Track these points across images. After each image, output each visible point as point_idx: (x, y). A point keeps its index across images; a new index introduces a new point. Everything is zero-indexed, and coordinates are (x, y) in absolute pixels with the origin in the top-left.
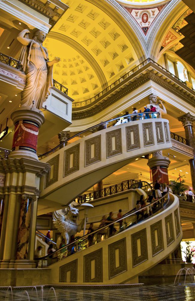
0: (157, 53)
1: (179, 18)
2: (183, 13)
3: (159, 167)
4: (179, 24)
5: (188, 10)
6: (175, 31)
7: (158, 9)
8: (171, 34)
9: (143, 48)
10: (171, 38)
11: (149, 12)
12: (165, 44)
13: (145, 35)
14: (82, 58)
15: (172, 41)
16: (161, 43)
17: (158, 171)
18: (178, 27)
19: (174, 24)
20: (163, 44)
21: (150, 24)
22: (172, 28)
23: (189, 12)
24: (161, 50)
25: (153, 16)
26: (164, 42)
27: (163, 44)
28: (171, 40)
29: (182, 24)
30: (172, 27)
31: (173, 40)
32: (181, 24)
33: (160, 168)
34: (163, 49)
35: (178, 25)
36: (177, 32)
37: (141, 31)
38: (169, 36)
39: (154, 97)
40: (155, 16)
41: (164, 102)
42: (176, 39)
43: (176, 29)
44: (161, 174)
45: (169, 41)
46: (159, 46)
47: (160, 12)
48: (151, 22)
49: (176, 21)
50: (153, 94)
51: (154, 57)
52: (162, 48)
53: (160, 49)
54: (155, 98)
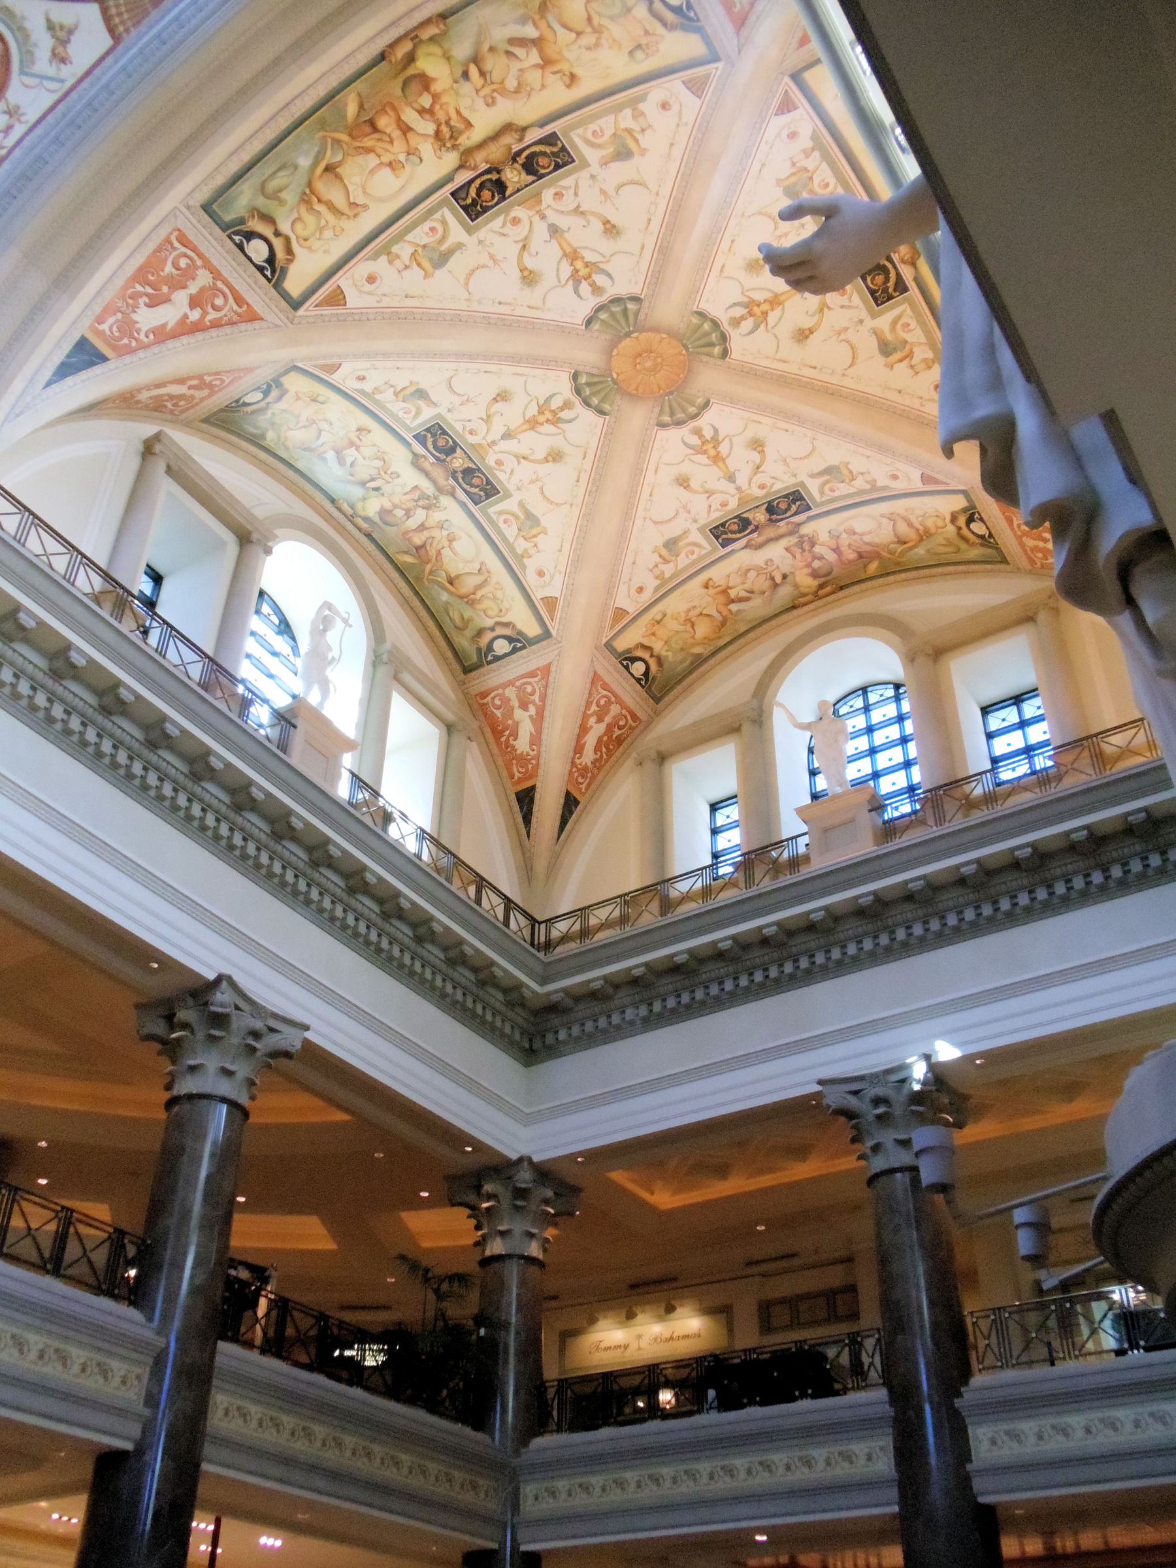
1: (270, 135)
2: (308, 102)
4: (275, 196)
5: (359, 85)
6: (241, 247)
7: (107, 19)
8: (192, 267)
10: (194, 302)
11: (27, 25)
12: (128, 327)
15: (198, 328)
16: (75, 308)
18: (269, 219)
19: (220, 180)
20: (100, 320)
21: (19, 130)
22: (206, 207)
23: (361, 107)
25: (51, 70)
26: (107, 311)
27: (100, 320)
28: (195, 315)
29: (305, 200)
30: (204, 195)
31: (216, 324)
32: (290, 196)
35: (261, 202)
36: (261, 269)
38: (169, 269)
40: (71, 73)
42: (243, 326)
43: (250, 235)
45: (168, 315)
47: (120, 48)
48: (32, 116)
49: (246, 157)
53: (58, 358)
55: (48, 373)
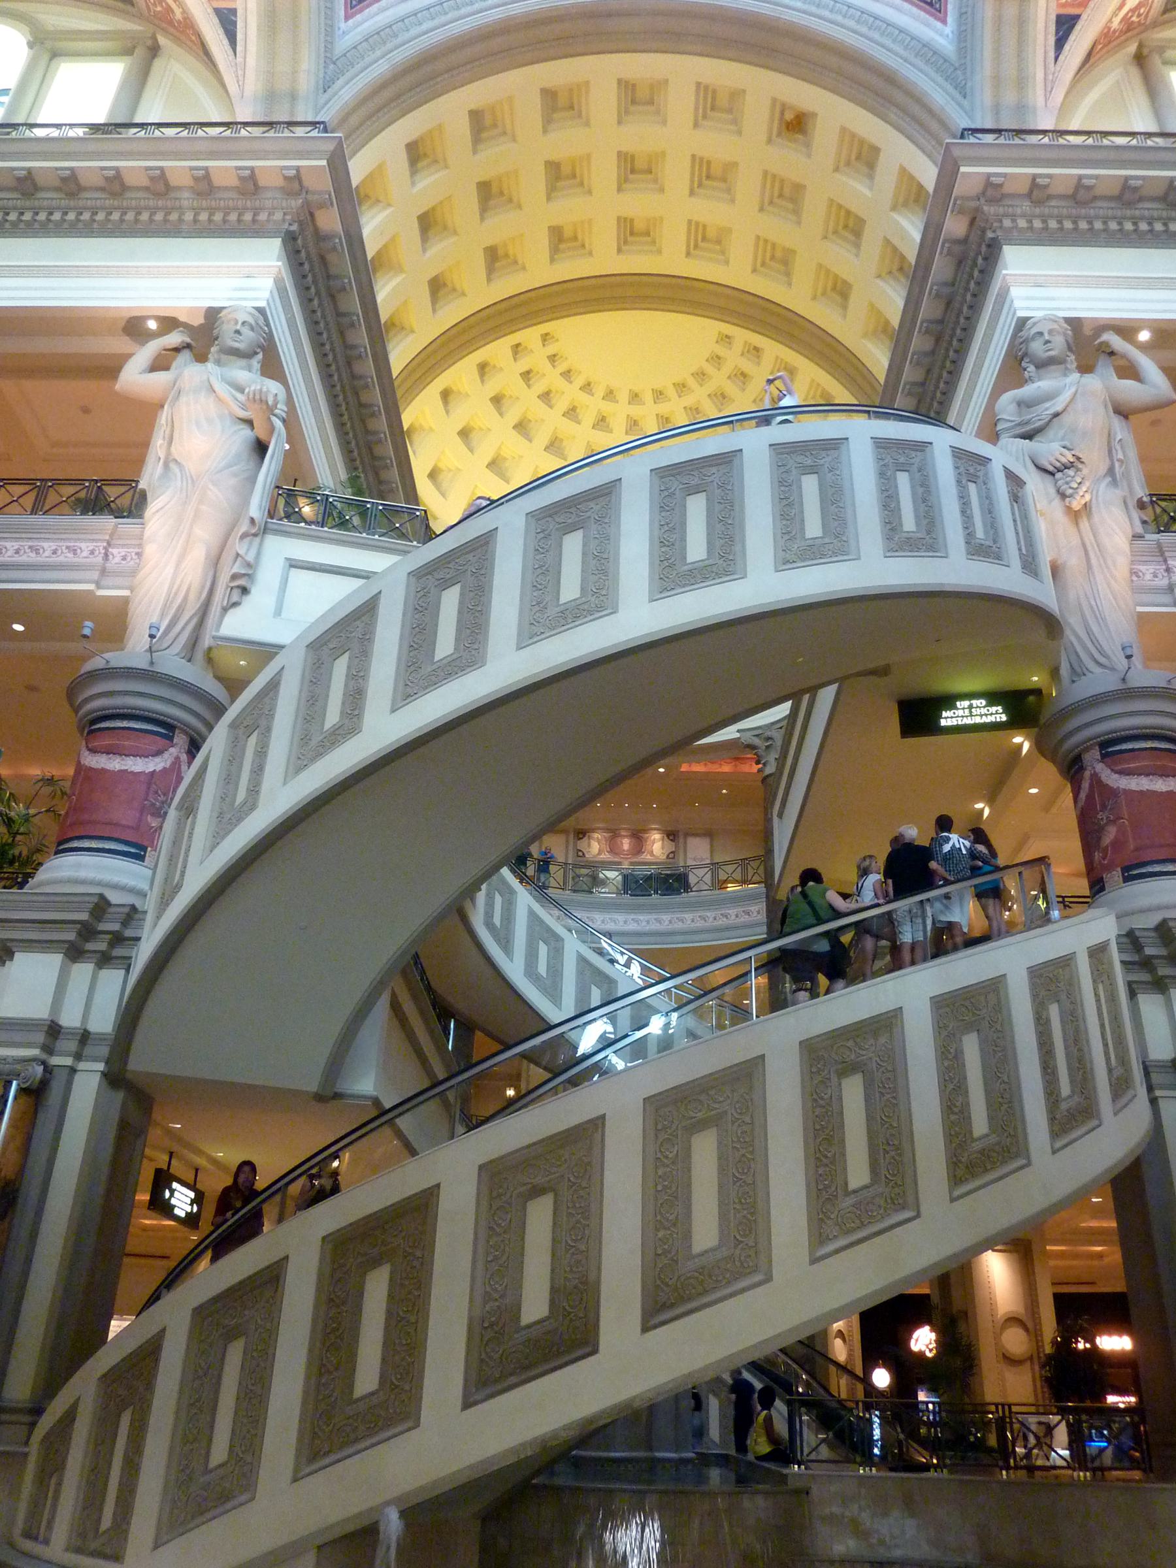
0: (1040, 75)
3: (1096, 753)
9: (938, 94)
13: (939, 25)
14: (741, 336)
17: (1091, 786)
24: (1060, 43)
33: (1104, 756)
34: (1078, 27)
37: (916, 18)
39: (1033, 331)
41: (1126, 330)
44: (1114, 793)
46: (1041, 25)
50: (1028, 319)
51: (1022, 108)
52: (1065, 25)
54: (1041, 334)
55: (1052, 54)
